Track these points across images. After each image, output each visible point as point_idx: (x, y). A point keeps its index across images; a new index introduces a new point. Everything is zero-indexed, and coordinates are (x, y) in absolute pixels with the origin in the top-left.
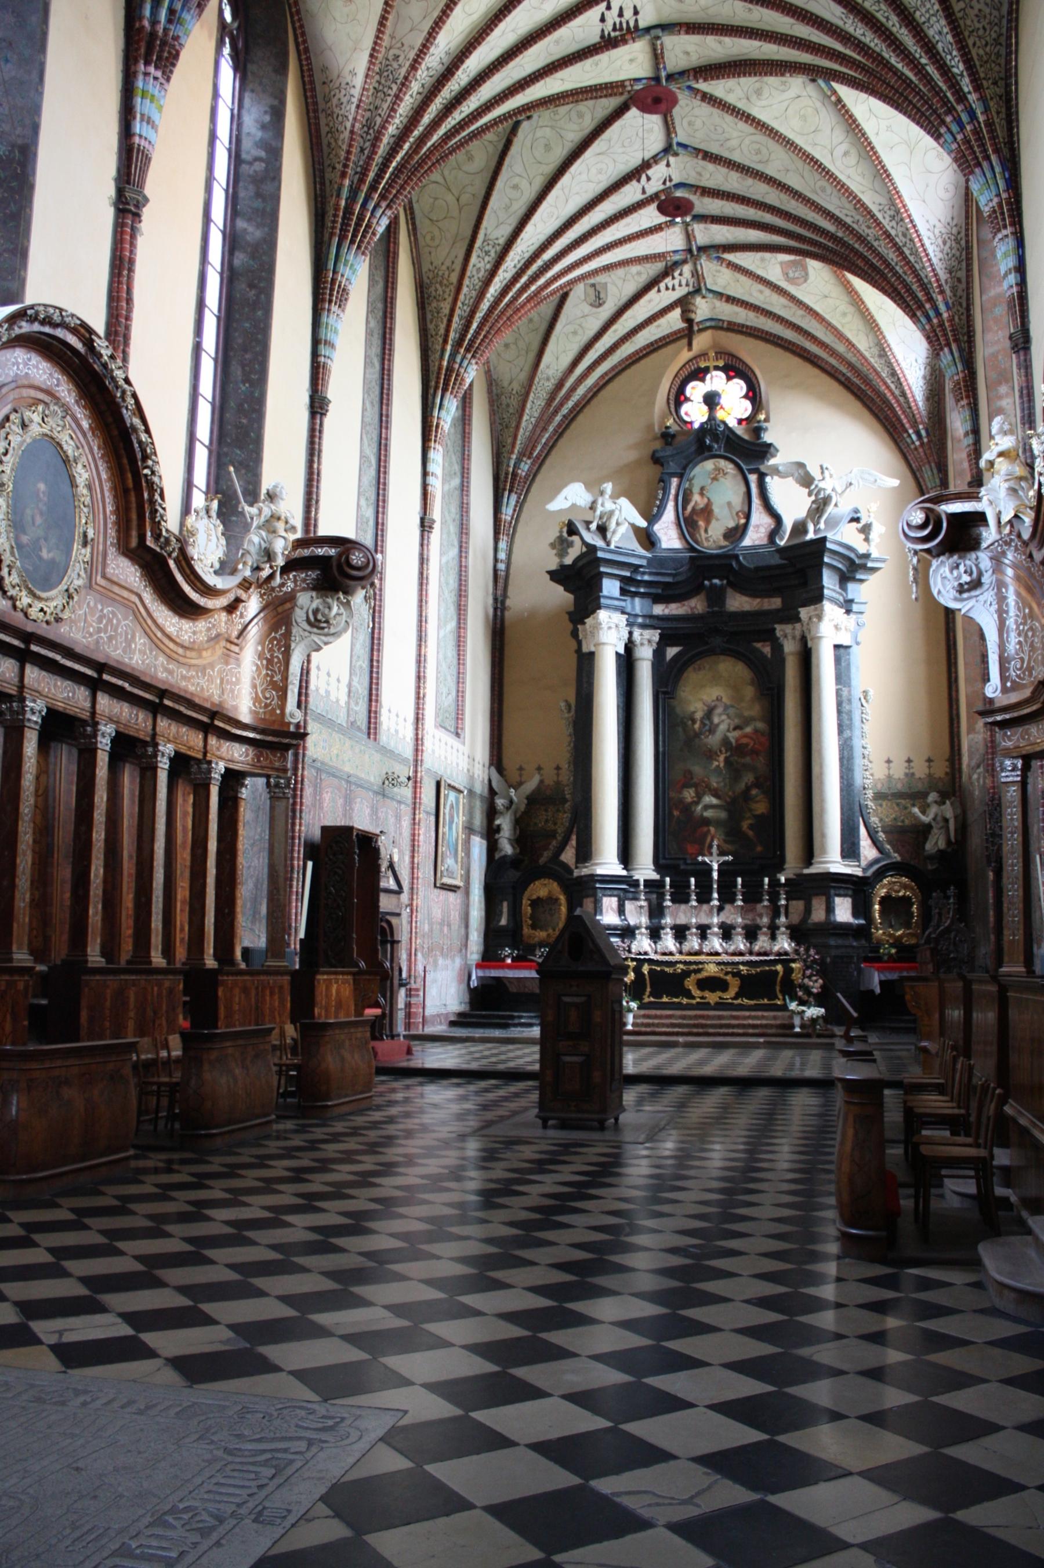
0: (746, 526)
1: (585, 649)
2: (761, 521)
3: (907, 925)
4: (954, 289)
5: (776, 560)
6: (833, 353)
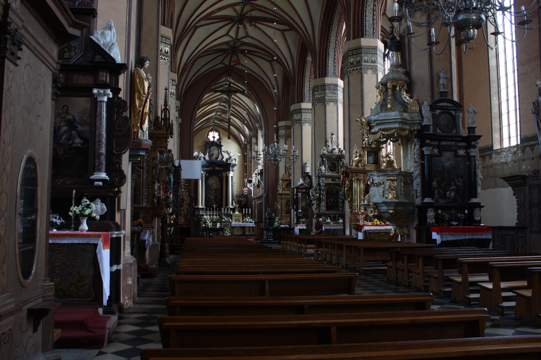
0: (218, 157)
2: (220, 156)
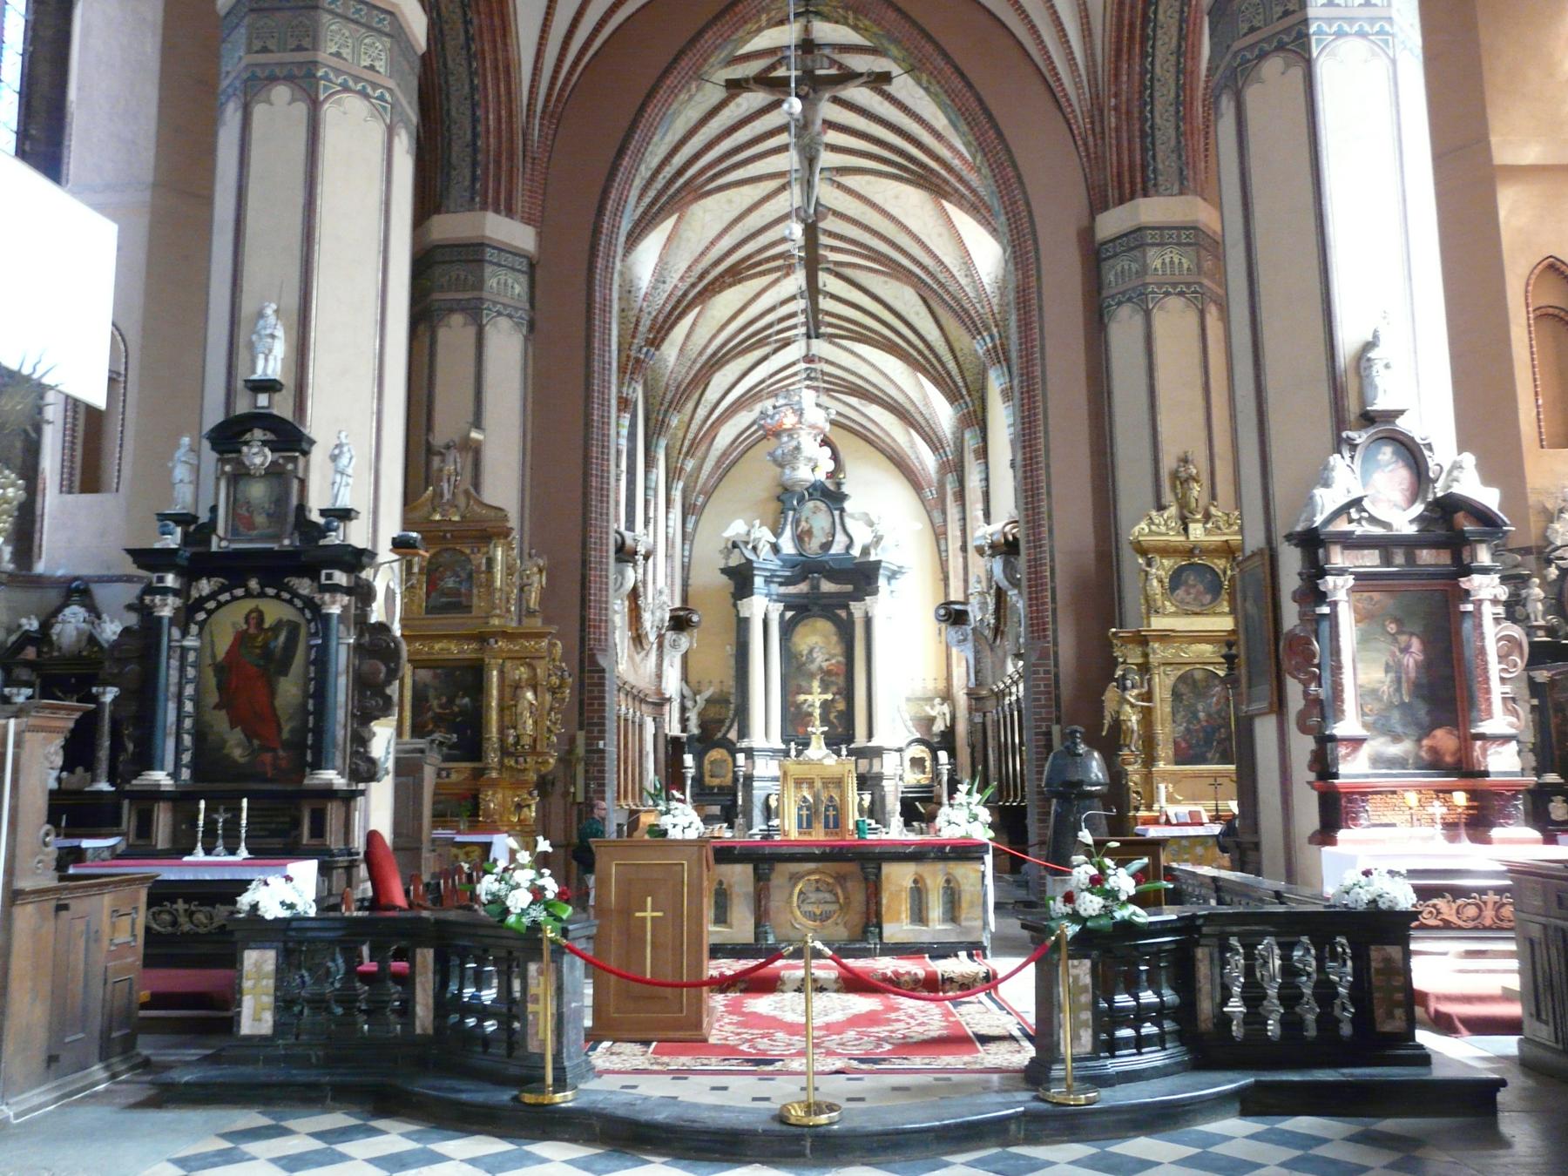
0: (832, 541)
1: (741, 615)
3: (924, 773)
4: (955, 443)
5: (850, 566)
6: (884, 442)
